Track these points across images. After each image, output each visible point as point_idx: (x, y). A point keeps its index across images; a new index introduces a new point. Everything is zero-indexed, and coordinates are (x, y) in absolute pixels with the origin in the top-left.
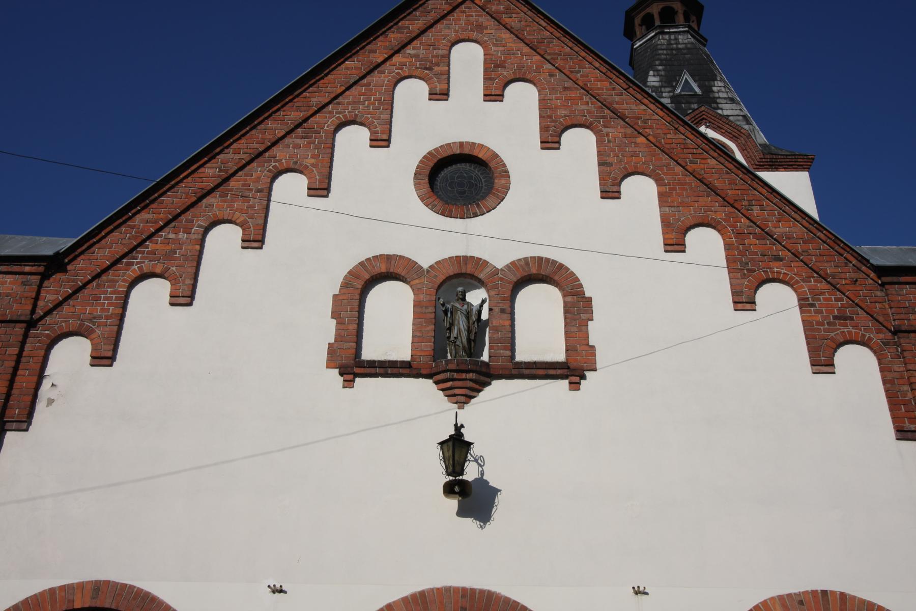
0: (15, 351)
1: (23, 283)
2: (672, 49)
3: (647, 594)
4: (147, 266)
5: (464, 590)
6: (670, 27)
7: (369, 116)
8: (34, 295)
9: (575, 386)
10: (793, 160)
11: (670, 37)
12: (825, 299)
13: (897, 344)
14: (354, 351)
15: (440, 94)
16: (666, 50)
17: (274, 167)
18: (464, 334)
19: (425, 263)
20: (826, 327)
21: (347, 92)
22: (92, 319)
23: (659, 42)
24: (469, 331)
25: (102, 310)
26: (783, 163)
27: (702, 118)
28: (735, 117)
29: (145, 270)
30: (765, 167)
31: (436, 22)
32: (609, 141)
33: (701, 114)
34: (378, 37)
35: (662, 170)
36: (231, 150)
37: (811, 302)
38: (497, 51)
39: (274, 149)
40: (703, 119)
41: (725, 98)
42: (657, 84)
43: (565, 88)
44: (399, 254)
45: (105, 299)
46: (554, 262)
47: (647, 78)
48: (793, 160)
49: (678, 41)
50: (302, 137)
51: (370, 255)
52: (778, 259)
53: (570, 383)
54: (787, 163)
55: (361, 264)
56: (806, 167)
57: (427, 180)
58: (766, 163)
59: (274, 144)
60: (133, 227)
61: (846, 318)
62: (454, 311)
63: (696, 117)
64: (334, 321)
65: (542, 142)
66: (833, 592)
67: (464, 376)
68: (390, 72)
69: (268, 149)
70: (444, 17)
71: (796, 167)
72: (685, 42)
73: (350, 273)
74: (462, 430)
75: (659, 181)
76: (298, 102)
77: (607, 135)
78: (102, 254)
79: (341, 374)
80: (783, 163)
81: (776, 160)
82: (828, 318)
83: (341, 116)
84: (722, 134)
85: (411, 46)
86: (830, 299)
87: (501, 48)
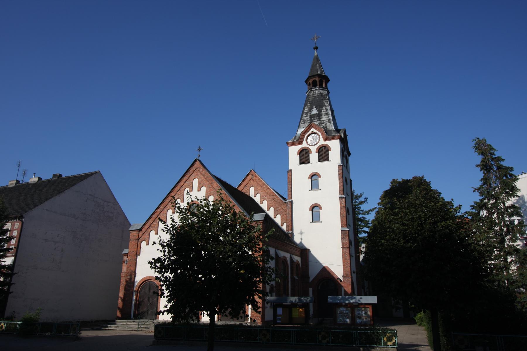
1: (137, 233)
2: (313, 97)
4: (152, 229)
31: (191, 175)
42: (307, 111)
43: (210, 187)
70: (192, 174)
78: (146, 227)
84: (317, 130)
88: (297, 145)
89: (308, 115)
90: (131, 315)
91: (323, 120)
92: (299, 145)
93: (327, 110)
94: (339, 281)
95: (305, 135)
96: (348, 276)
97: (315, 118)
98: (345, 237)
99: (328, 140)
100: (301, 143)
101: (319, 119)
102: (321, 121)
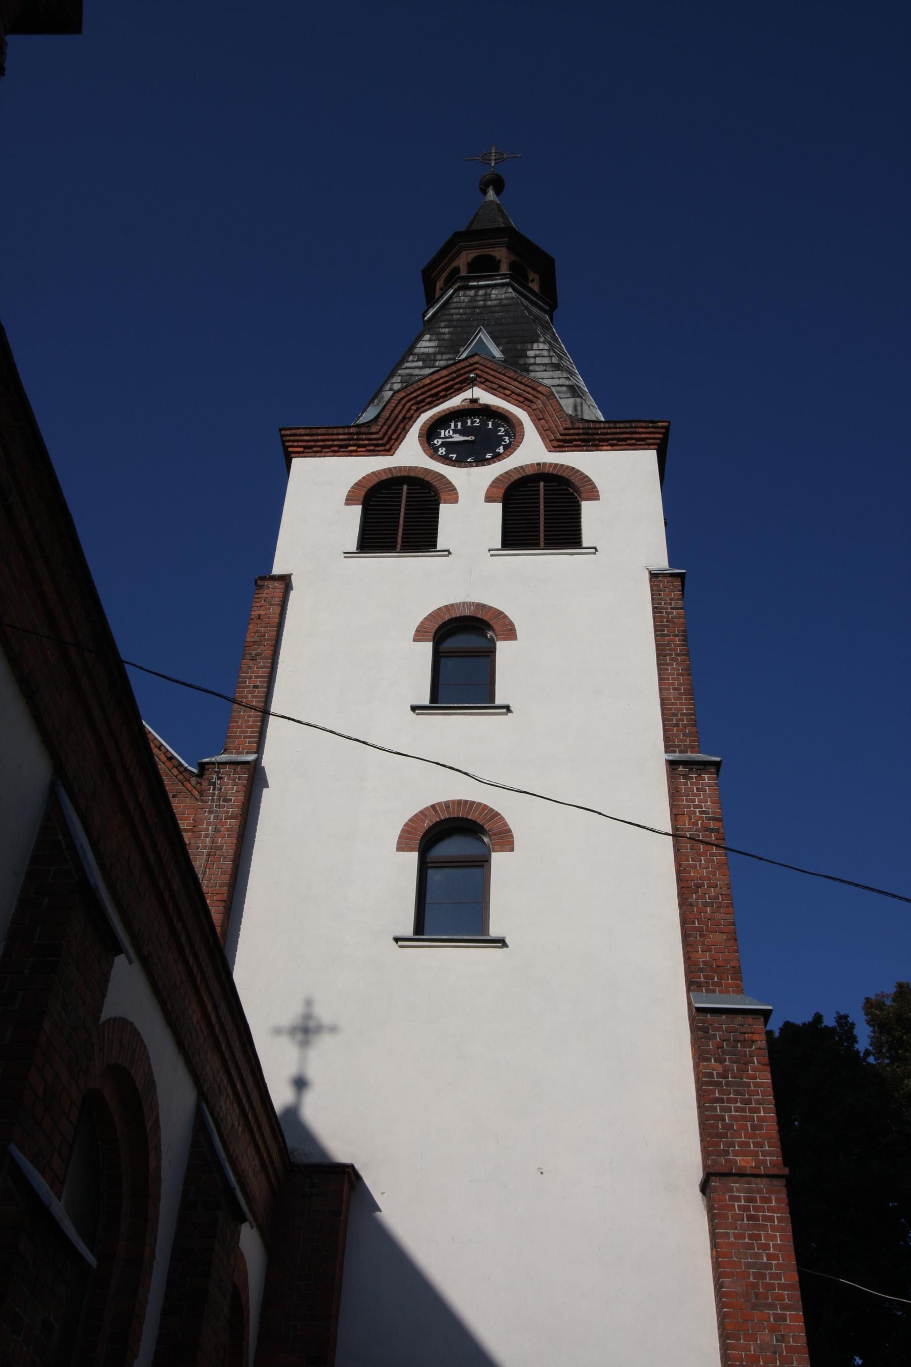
2: (475, 308)
30: (575, 443)
56: (651, 441)
81: (594, 431)
84: (506, 398)
88: (350, 454)
95: (420, 411)
98: (743, 1070)
100: (388, 446)
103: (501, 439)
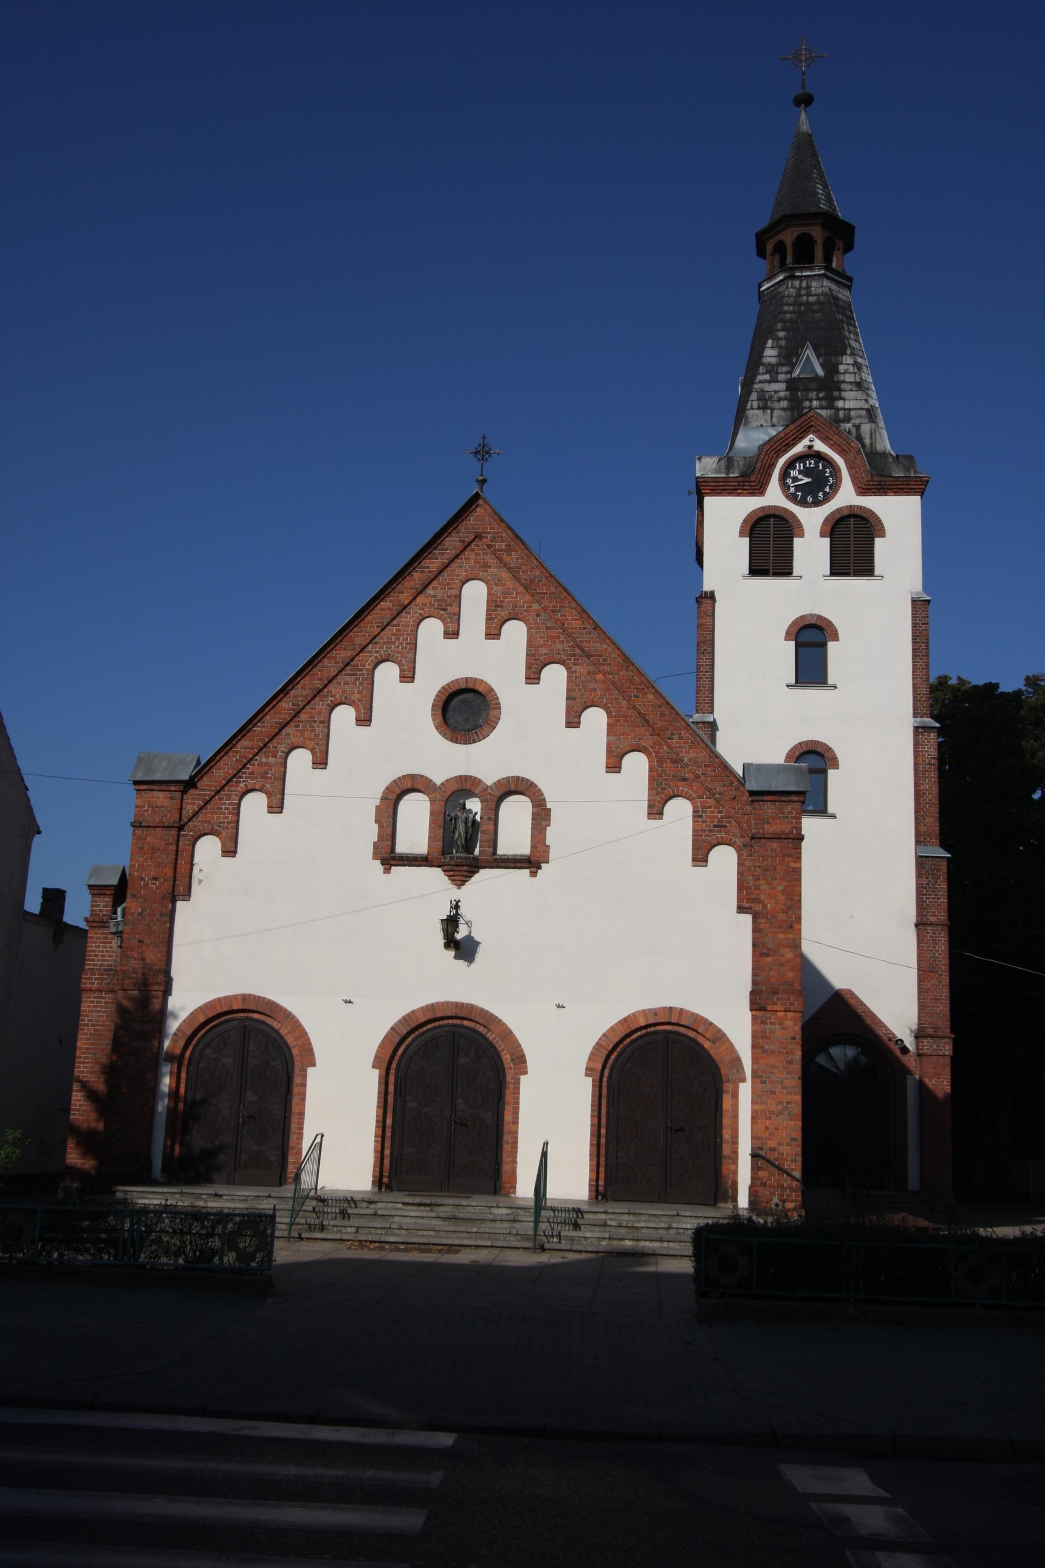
0: (174, 847)
1: (171, 798)
2: (800, 304)
3: (564, 1007)
4: (250, 783)
5: (457, 1003)
6: (802, 269)
7: (398, 655)
8: (179, 806)
9: (534, 874)
10: (905, 483)
11: (801, 283)
12: (710, 812)
13: (751, 846)
14: (390, 848)
15: (452, 633)
16: (793, 305)
17: (331, 701)
18: (463, 836)
19: (438, 780)
20: (707, 833)
21: (383, 632)
22: (219, 824)
23: (786, 293)
24: (466, 833)
25: (225, 818)
26: (892, 487)
27: (810, 425)
28: (857, 411)
29: (249, 787)
30: (873, 490)
31: (451, 561)
32: (576, 678)
33: (809, 421)
34: (406, 577)
35: (612, 703)
36: (299, 686)
37: (700, 814)
38: (498, 590)
39: (330, 685)
40: (812, 426)
41: (851, 383)
42: (773, 361)
43: (548, 628)
44: (420, 773)
45: (226, 809)
46: (528, 780)
47: (763, 351)
48: (905, 483)
49: (811, 291)
50: (350, 675)
51: (400, 775)
52: (684, 780)
53: (531, 872)
54: (898, 487)
55: (395, 781)
56: (918, 490)
57: (440, 712)
58: (874, 487)
59: (330, 681)
60: (237, 752)
61: (721, 826)
62: (456, 818)
63: (803, 425)
64: (377, 825)
65: (526, 679)
66: (676, 1008)
67: (460, 868)
68: (414, 613)
69: (326, 686)
70: (457, 556)
71: (907, 490)
72: (818, 292)
73: (387, 788)
74: (459, 904)
75: (609, 716)
76: (344, 644)
77: (575, 672)
78: (220, 774)
79: (382, 864)
80: (892, 487)
81: (885, 483)
82: (710, 826)
83: (378, 655)
84: (831, 446)
85: (431, 586)
86: (714, 812)
87: (501, 588)
88: (739, 495)
89: (781, 377)
90: (149, 1162)
91: (847, 407)
92: (752, 494)
93: (858, 366)
94: (898, 1052)
95: (778, 457)
96: (940, 1034)
97: (810, 395)
99: (875, 494)
100: (759, 489)
101: (830, 401)
102: (838, 409)
103: (827, 479)
